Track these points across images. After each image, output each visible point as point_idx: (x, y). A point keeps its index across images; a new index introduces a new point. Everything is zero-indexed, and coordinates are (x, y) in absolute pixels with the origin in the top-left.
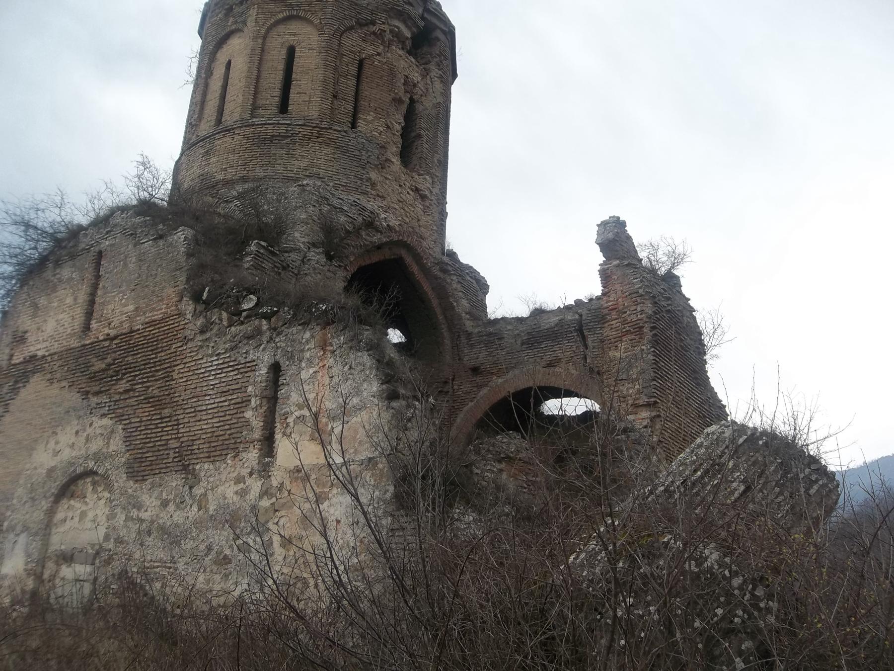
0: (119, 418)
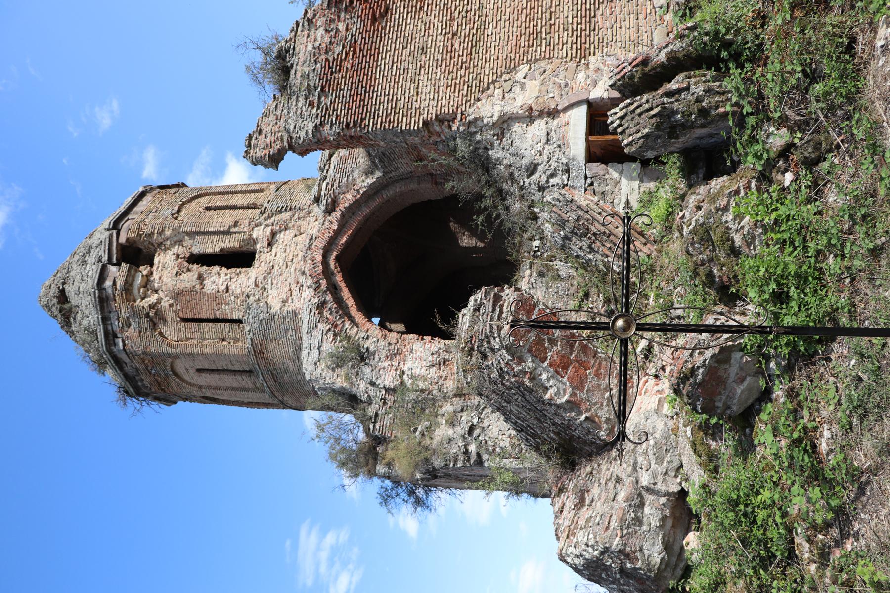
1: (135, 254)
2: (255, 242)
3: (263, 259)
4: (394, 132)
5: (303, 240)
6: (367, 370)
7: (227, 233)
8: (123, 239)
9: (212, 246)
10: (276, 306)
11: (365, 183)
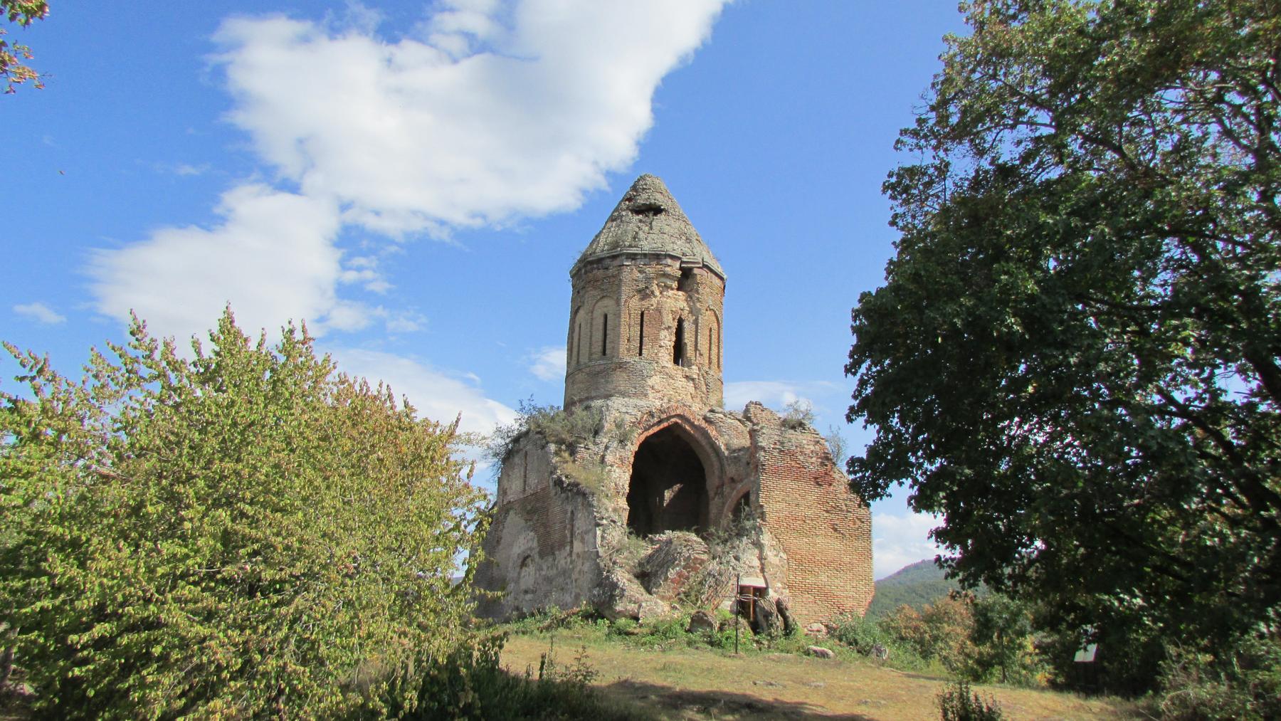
0: (536, 532)
1: (686, 278)
2: (689, 366)
3: (677, 371)
4: (758, 489)
5: (689, 401)
6: (615, 444)
7: (696, 349)
8: (696, 271)
9: (688, 338)
10: (650, 382)
11: (721, 443)
